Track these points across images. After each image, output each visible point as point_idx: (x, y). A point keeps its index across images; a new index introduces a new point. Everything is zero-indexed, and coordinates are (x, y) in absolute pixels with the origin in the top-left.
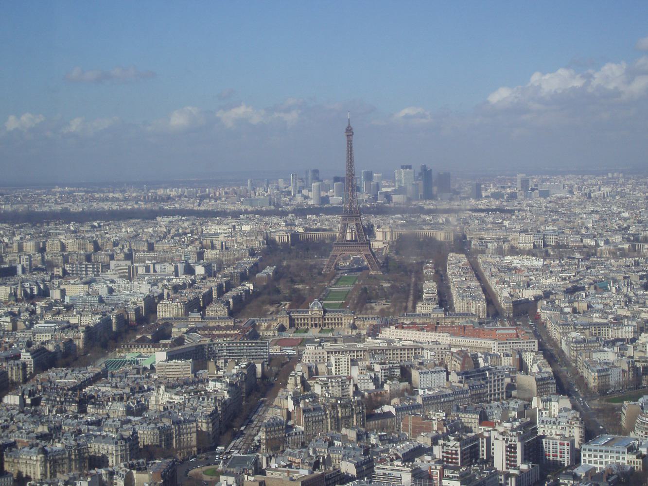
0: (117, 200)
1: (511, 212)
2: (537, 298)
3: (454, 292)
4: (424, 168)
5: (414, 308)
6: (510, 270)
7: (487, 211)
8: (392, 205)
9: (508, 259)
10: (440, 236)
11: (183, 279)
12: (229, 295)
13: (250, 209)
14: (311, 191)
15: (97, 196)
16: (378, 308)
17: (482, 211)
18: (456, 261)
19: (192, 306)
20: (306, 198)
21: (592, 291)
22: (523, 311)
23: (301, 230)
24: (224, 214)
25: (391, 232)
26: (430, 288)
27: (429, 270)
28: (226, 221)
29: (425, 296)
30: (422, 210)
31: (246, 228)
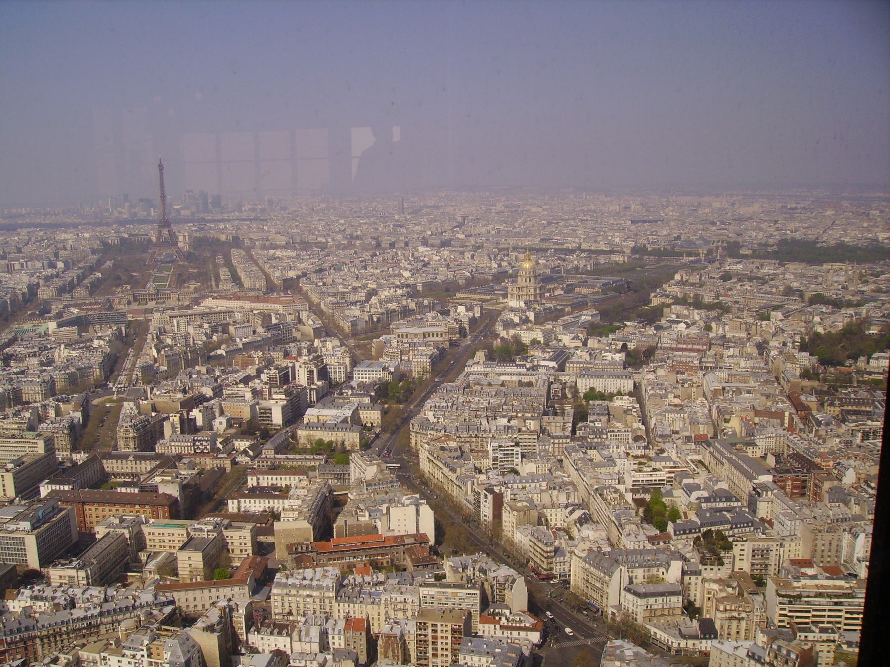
2: (299, 277)
3: (242, 275)
5: (217, 286)
16: (192, 287)
19: (61, 291)
21: (332, 271)
22: (290, 285)
29: (222, 278)
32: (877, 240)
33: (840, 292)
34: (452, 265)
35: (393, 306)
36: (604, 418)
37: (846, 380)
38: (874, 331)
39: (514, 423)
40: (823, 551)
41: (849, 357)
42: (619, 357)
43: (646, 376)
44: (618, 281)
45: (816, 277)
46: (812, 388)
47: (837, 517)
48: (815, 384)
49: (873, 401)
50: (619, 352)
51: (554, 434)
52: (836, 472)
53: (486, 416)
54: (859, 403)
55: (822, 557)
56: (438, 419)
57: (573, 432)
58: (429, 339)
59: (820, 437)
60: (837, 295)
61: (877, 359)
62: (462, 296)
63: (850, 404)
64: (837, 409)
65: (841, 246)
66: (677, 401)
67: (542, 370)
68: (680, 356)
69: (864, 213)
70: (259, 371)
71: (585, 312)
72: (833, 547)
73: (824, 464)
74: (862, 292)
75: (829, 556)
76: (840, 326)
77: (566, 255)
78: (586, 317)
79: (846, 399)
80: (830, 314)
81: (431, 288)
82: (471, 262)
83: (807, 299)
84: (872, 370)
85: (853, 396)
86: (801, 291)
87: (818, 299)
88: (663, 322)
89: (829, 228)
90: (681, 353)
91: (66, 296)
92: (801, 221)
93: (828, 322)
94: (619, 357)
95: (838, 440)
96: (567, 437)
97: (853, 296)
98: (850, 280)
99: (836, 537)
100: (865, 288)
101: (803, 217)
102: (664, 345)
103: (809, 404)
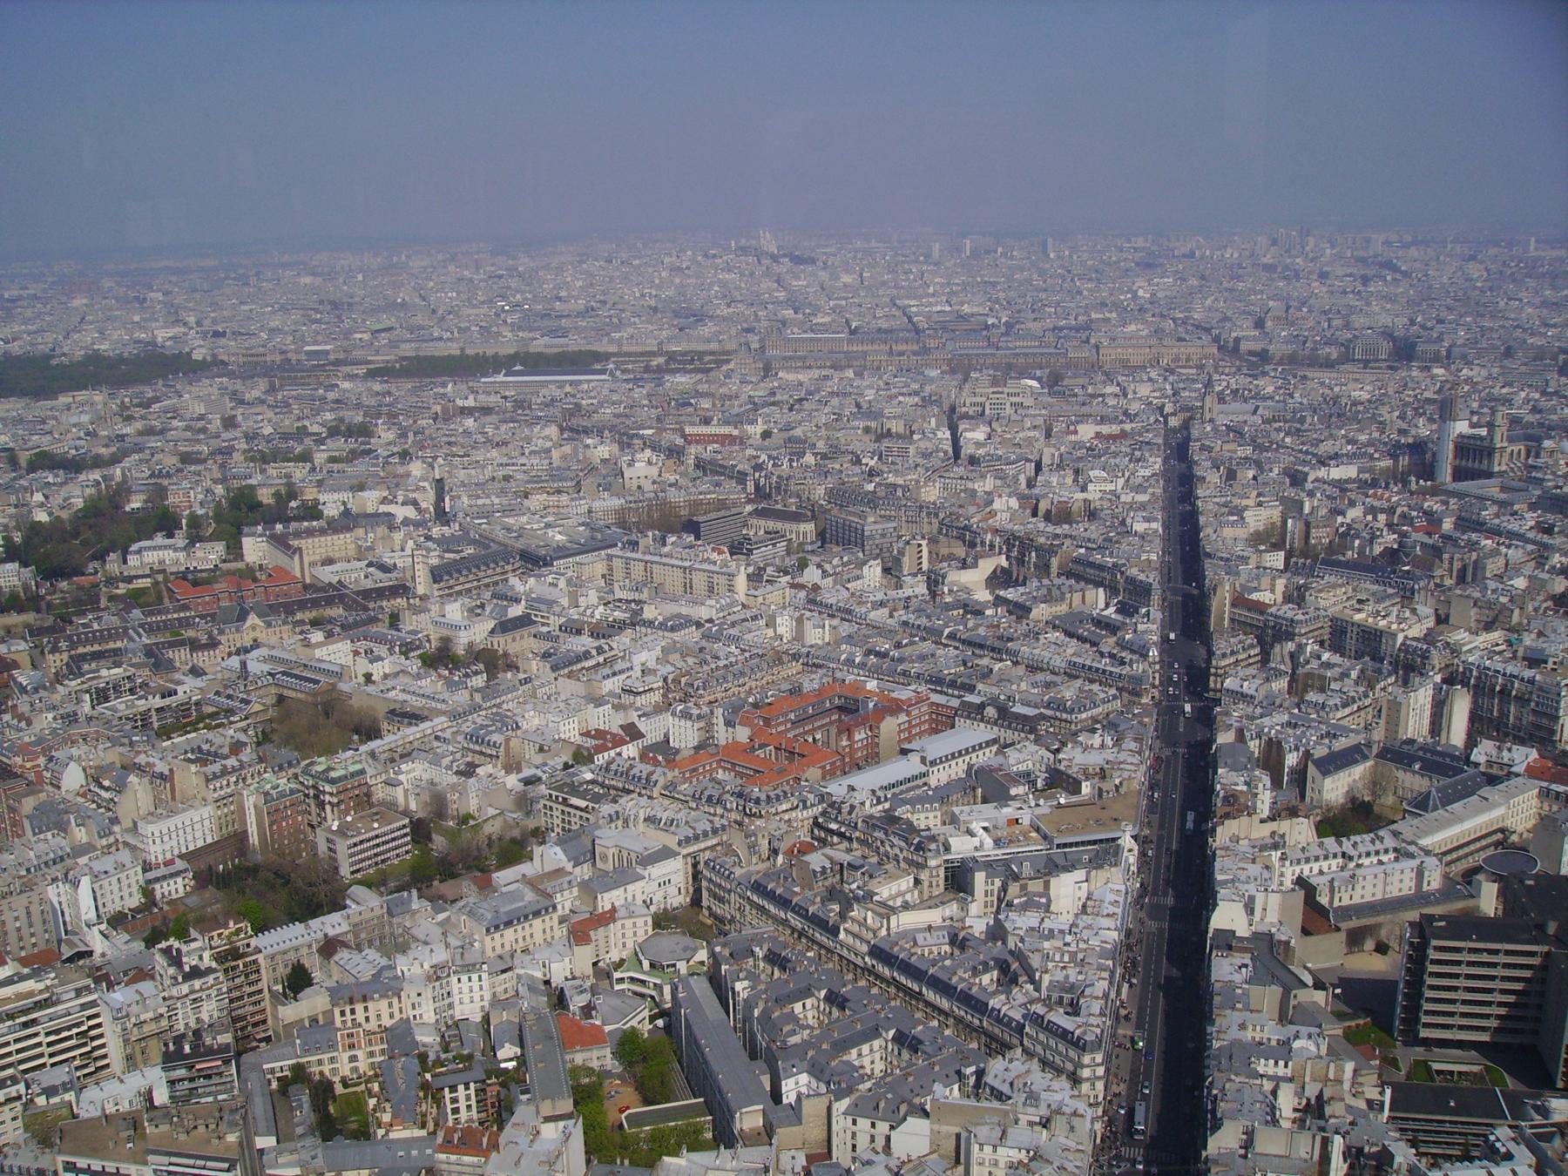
32: (154, 344)
33: (82, 443)
37: (88, 601)
38: (136, 503)
40: (19, 929)
41: (94, 558)
45: (43, 422)
46: (27, 626)
47: (45, 858)
48: (30, 617)
49: (126, 629)
52: (49, 775)
54: (102, 636)
55: (21, 939)
59: (21, 717)
60: (77, 449)
61: (139, 552)
63: (87, 642)
64: (65, 656)
65: (95, 359)
69: (137, 298)
72: (37, 918)
73: (28, 765)
74: (121, 438)
75: (32, 935)
76: (79, 503)
79: (86, 634)
80: (61, 484)
83: (23, 463)
84: (133, 573)
85: (96, 626)
86: (11, 450)
87: (44, 461)
89: (75, 330)
92: (26, 321)
93: (57, 500)
95: (50, 716)
97: (107, 446)
98: (100, 419)
99: (35, 899)
100: (127, 430)
101: (29, 313)
103: (13, 657)
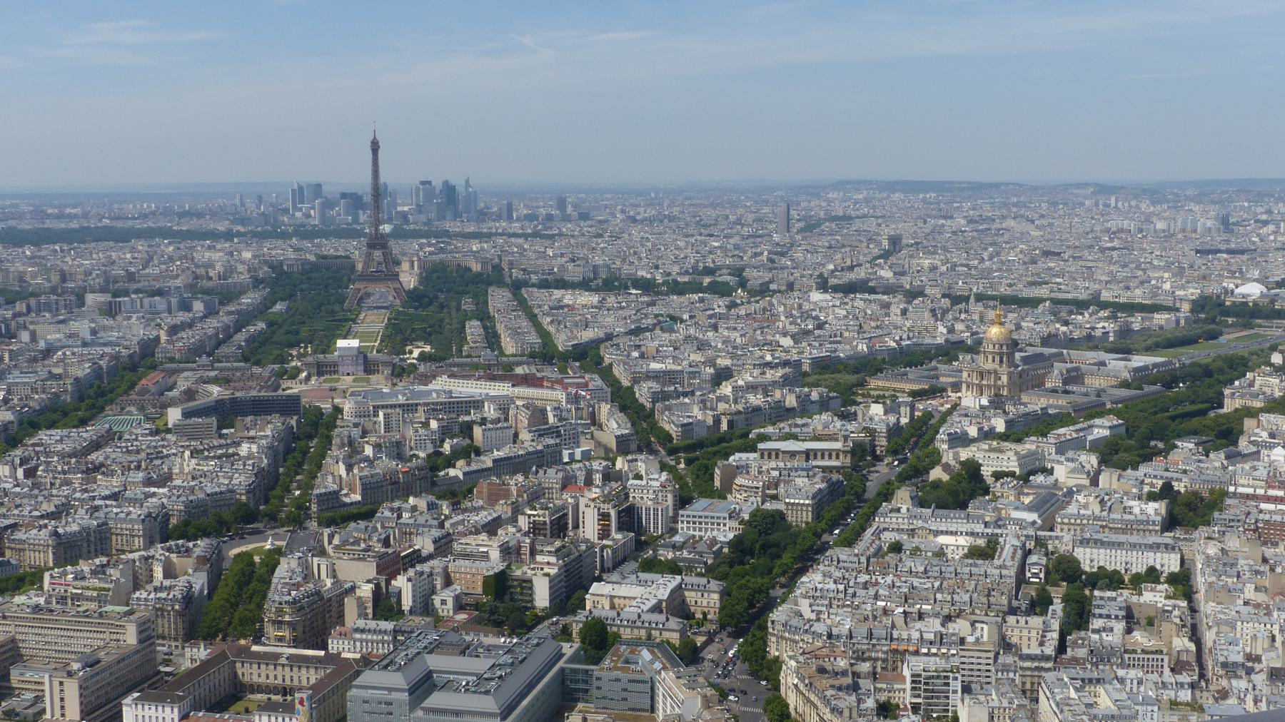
0: (76, 216)
1: (552, 237)
4: (446, 184)
6: (562, 307)
7: (526, 236)
8: (412, 227)
9: (557, 293)
10: (476, 267)
11: (182, 317)
12: (241, 338)
13: (242, 230)
14: (313, 208)
15: (50, 211)
16: (416, 353)
17: (515, 235)
18: (498, 299)
20: (308, 216)
21: (658, 331)
23: (312, 258)
24: (214, 236)
25: (419, 260)
26: (473, 329)
27: (468, 304)
28: (219, 246)
30: (446, 233)
31: (247, 255)
34: (866, 328)
35: (756, 400)
36: (1119, 627)
39: (953, 627)
42: (1156, 509)
43: (1203, 548)
44: (1162, 364)
50: (1152, 497)
51: (1025, 651)
53: (905, 612)
56: (819, 612)
57: (1062, 648)
58: (815, 463)
62: (880, 383)
66: (1261, 598)
67: (1012, 529)
68: (1270, 512)
70: (517, 511)
71: (1097, 421)
77: (1071, 313)
78: (1101, 429)
81: (825, 366)
82: (898, 320)
88: (1243, 444)
90: (1271, 507)
91: (204, 360)
94: (1156, 509)
96: (1047, 658)
102: (1240, 490)
